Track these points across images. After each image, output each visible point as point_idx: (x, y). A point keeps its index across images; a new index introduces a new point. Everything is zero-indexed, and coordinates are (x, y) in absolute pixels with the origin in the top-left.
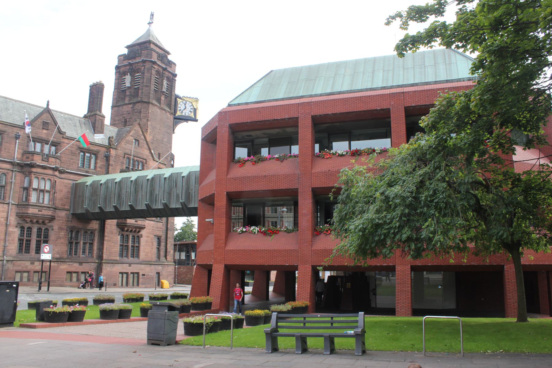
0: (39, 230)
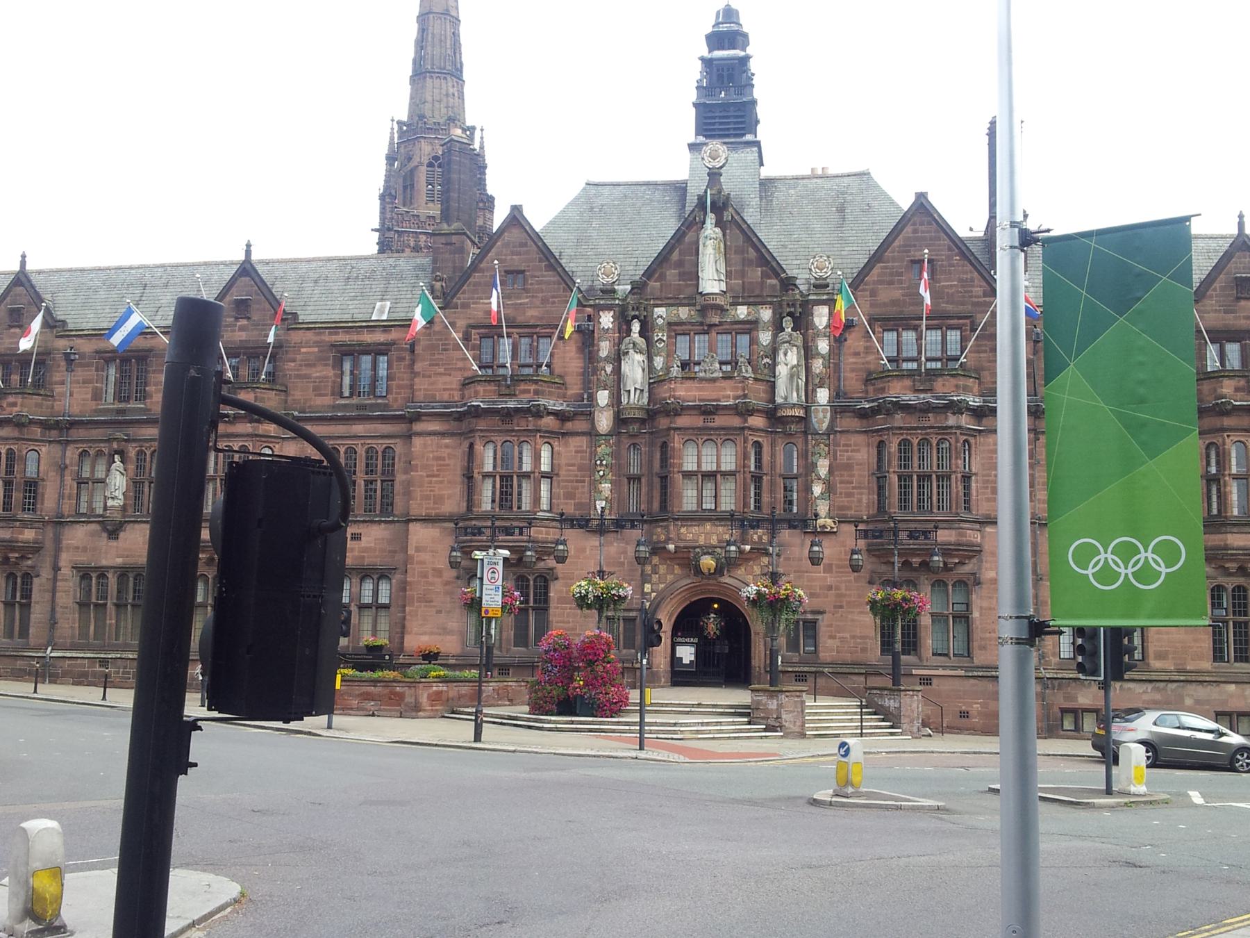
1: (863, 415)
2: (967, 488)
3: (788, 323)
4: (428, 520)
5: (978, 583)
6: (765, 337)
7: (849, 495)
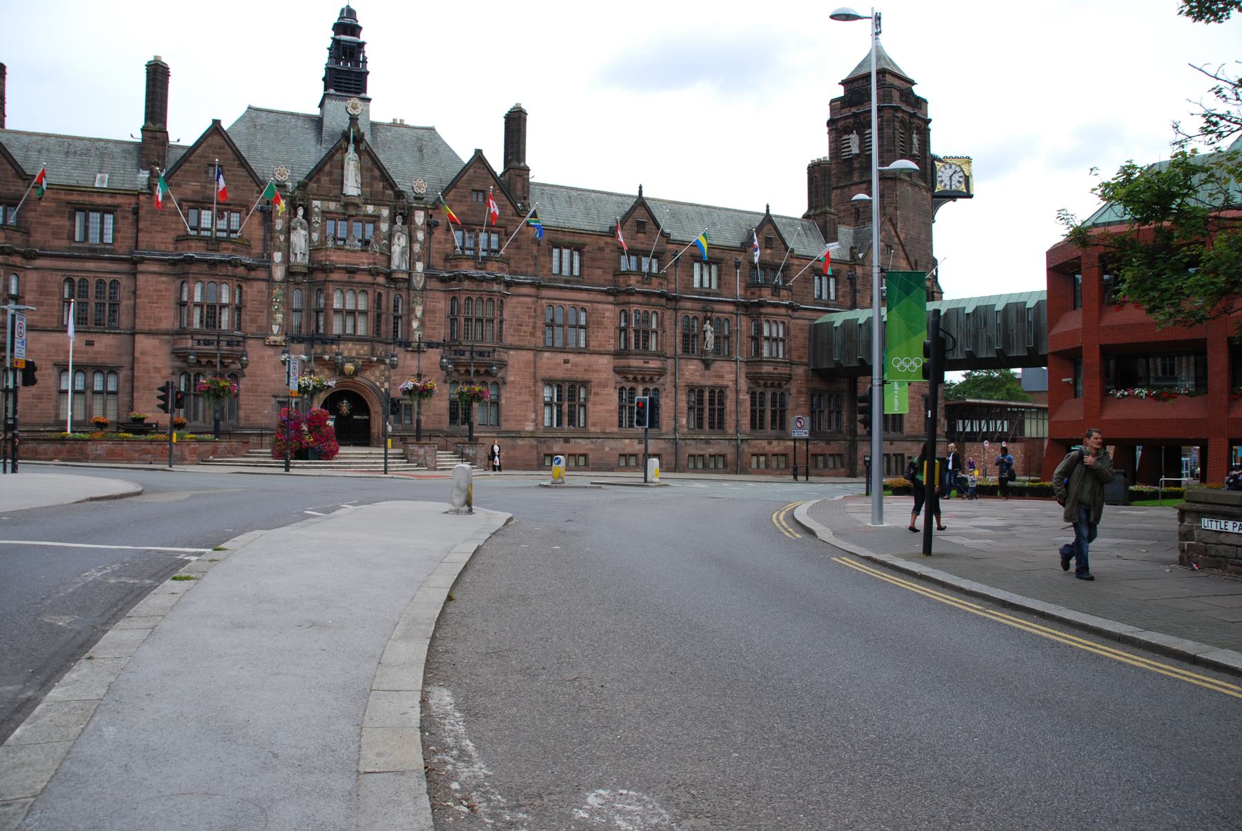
0: (774, 394)
1: (443, 280)
2: (501, 328)
3: (399, 219)
4: (149, 333)
5: (505, 383)
6: (384, 227)
7: (433, 329)
